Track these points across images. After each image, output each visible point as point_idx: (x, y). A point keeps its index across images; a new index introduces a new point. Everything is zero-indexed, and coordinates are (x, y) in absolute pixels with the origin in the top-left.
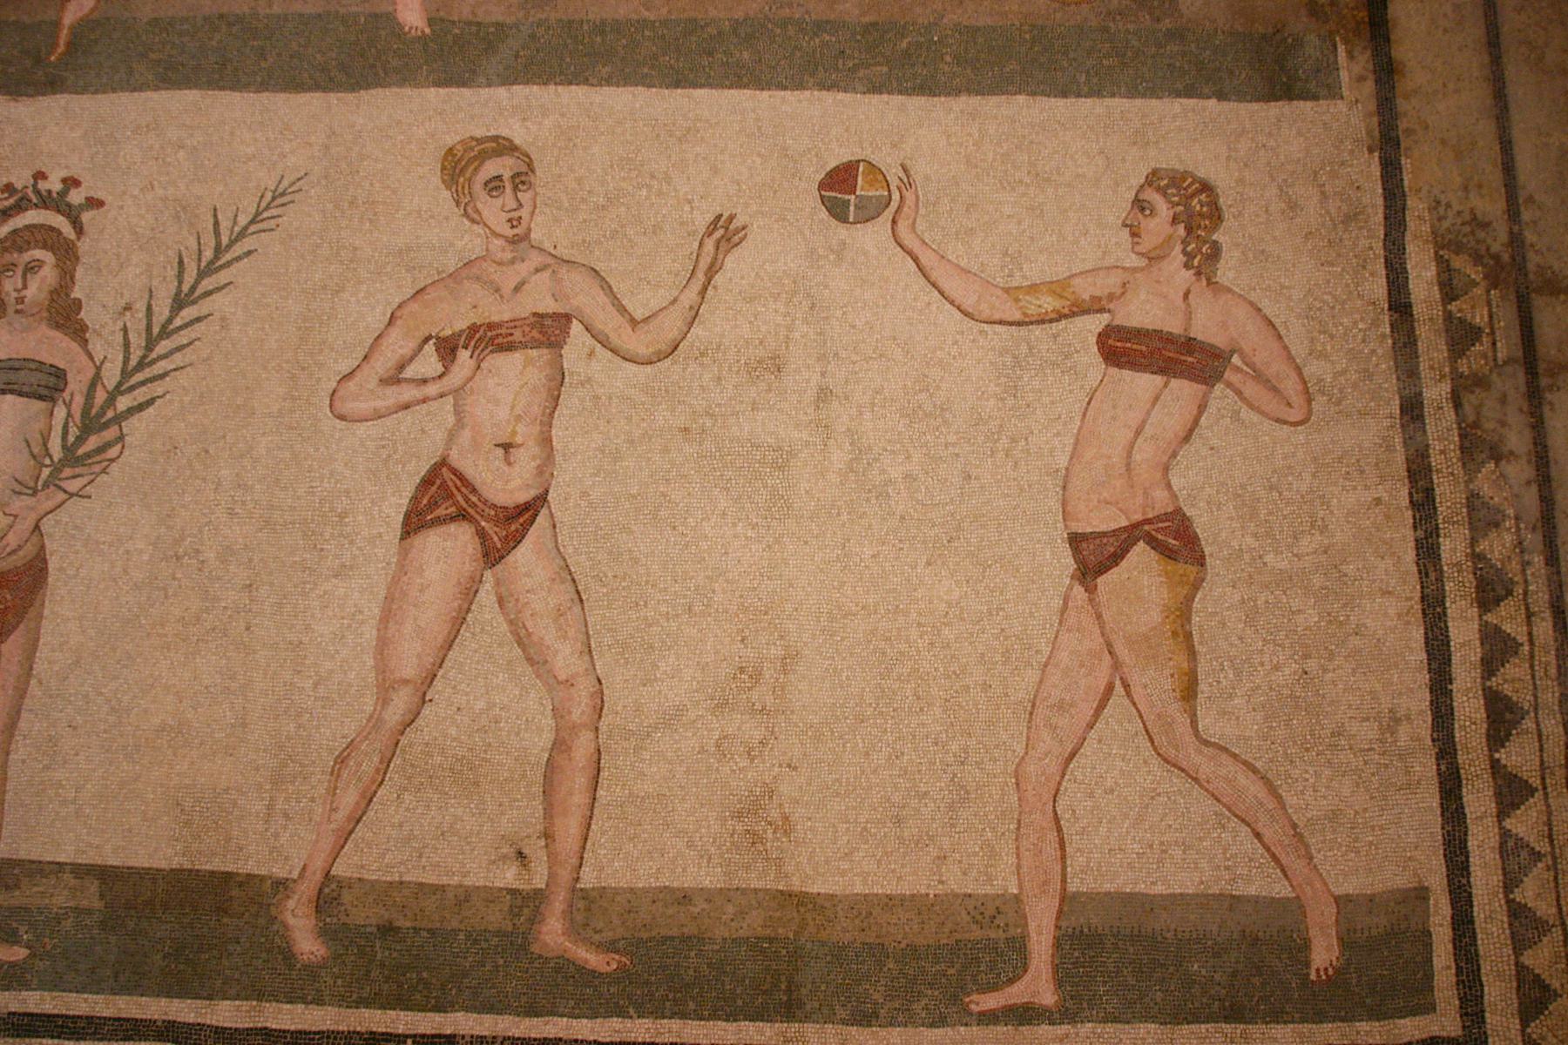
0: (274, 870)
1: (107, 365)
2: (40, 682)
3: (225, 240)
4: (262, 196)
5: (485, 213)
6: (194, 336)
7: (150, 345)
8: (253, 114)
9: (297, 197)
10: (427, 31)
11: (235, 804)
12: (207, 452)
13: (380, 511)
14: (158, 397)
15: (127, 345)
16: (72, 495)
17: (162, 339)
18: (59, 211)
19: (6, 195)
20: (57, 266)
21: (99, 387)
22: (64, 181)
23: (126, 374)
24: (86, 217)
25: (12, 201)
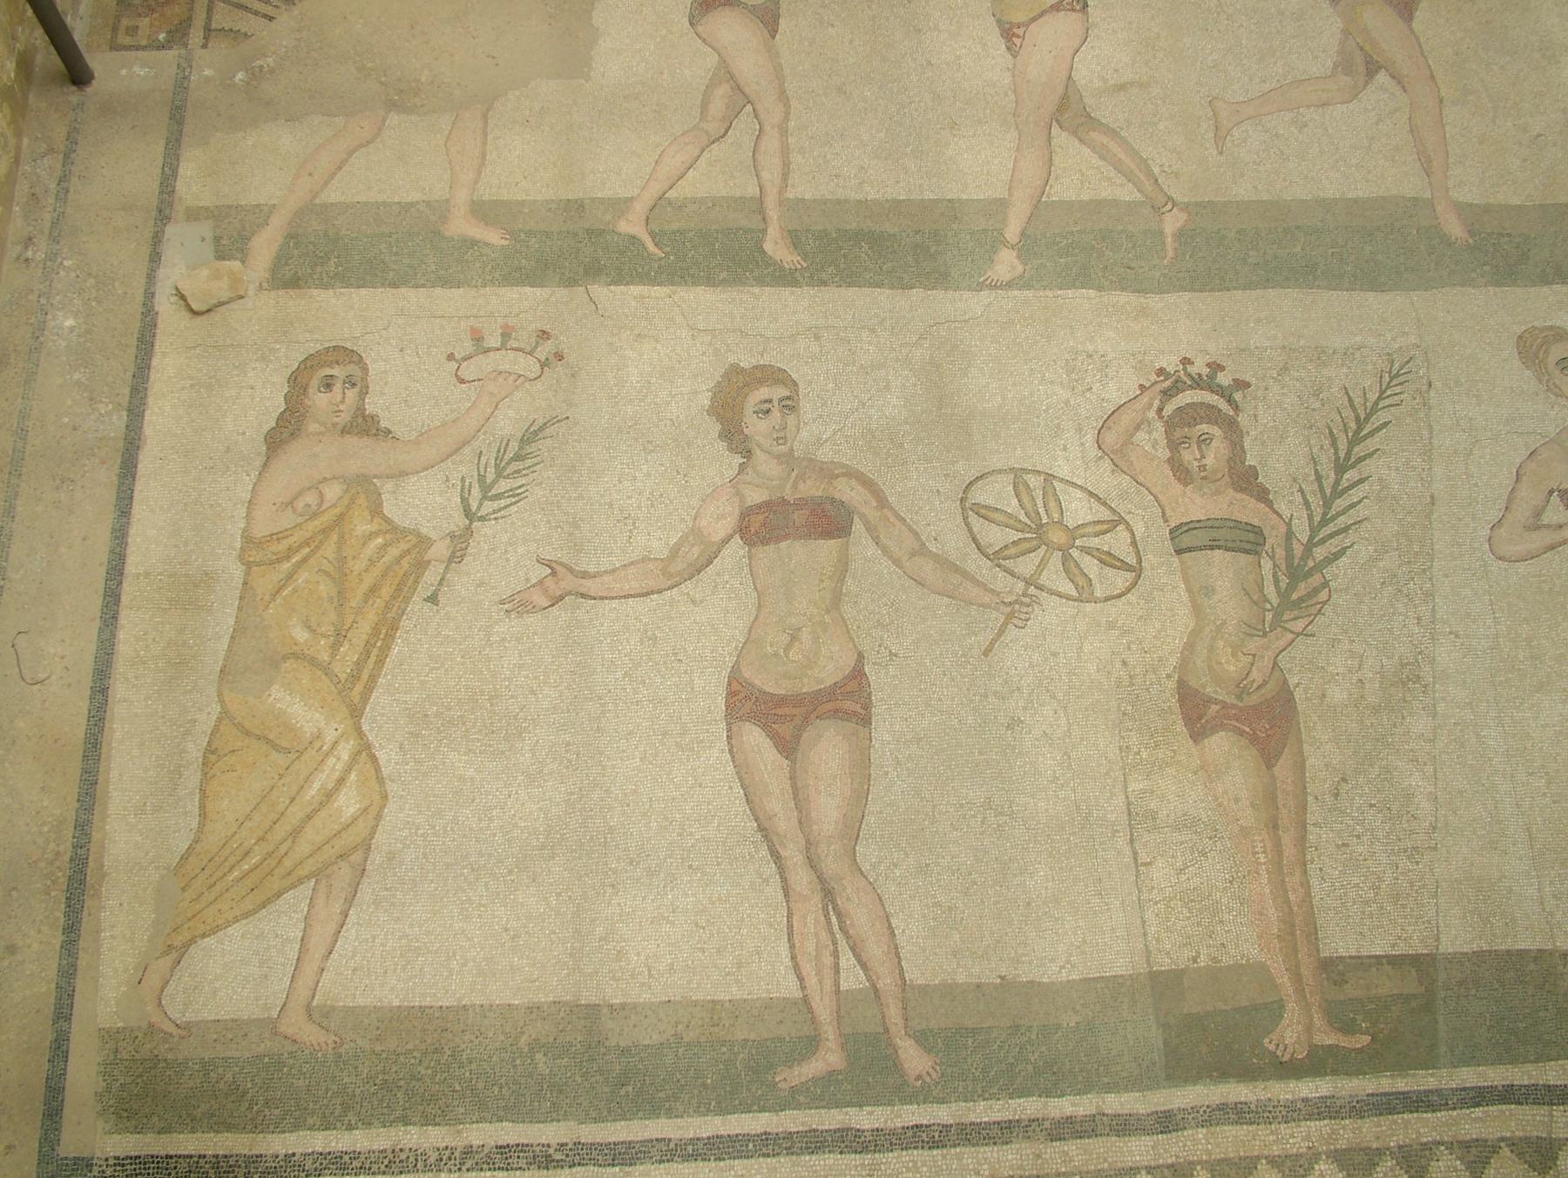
0: (1558, 944)
1: (1295, 522)
2: (1316, 798)
3: (1362, 416)
4: (1381, 377)
5: (1563, 388)
6: (1361, 495)
7: (1327, 505)
8: (1351, 308)
9: (1410, 377)
10: (1471, 241)
11: (1510, 891)
12: (1400, 591)
13: (1558, 635)
14: (1347, 547)
15: (1307, 503)
16: (1298, 634)
17: (1335, 498)
18: (1212, 392)
19: (1162, 378)
20: (1226, 438)
21: (1295, 541)
22: (1208, 365)
23: (1314, 531)
24: (1237, 396)
25: (1168, 383)
